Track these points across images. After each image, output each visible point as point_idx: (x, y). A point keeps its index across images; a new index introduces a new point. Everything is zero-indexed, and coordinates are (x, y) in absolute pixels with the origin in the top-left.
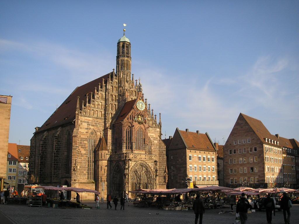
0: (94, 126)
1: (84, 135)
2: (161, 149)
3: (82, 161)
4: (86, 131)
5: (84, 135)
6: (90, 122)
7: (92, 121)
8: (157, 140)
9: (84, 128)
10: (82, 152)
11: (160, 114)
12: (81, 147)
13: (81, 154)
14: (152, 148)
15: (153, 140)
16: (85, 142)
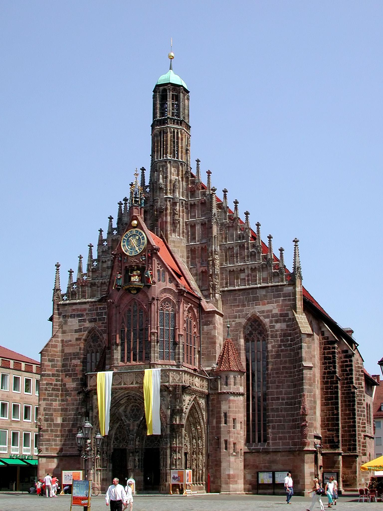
0: (94, 320)
1: (72, 345)
2: (296, 344)
3: (67, 405)
4: (77, 335)
5: (72, 345)
6: (85, 313)
7: (90, 310)
8: (284, 321)
9: (71, 331)
10: (67, 386)
11: (296, 241)
12: (66, 375)
13: (66, 390)
14: (270, 346)
15: (271, 322)
16: (75, 362)
